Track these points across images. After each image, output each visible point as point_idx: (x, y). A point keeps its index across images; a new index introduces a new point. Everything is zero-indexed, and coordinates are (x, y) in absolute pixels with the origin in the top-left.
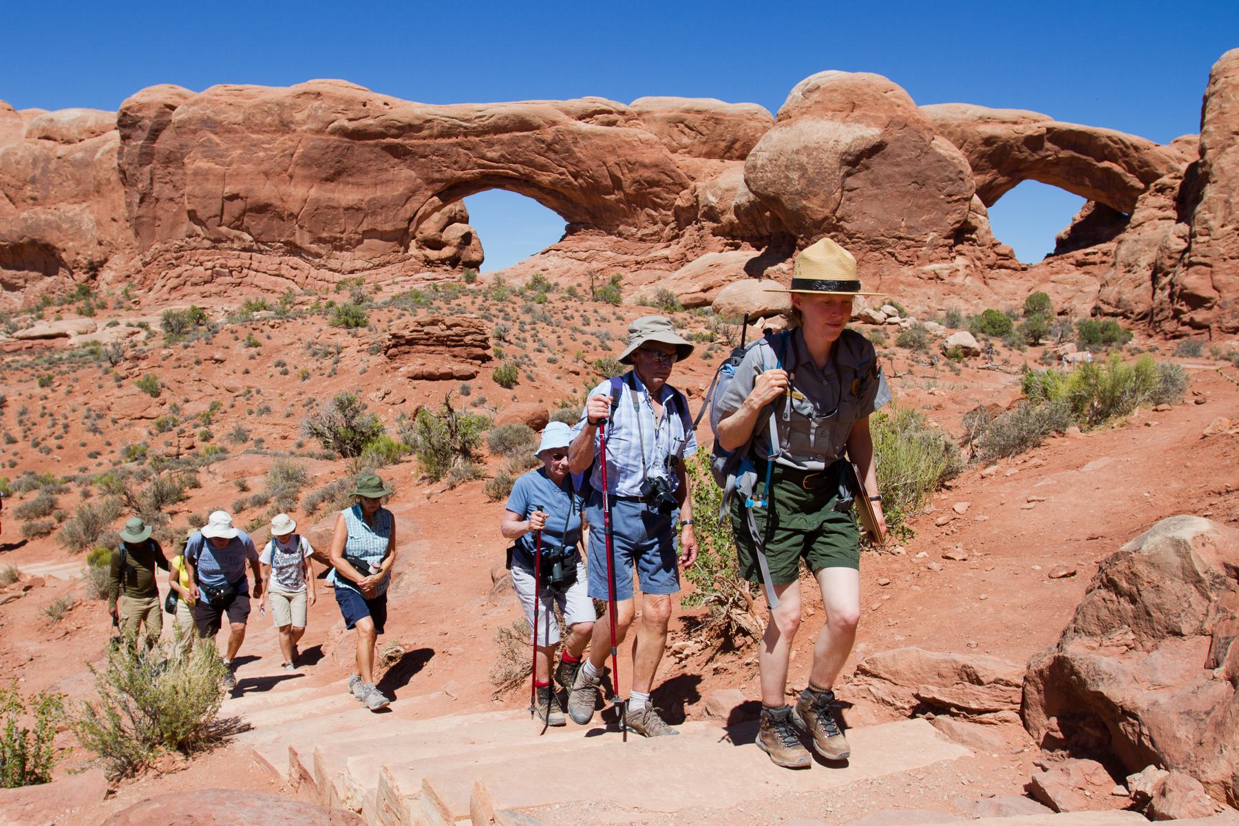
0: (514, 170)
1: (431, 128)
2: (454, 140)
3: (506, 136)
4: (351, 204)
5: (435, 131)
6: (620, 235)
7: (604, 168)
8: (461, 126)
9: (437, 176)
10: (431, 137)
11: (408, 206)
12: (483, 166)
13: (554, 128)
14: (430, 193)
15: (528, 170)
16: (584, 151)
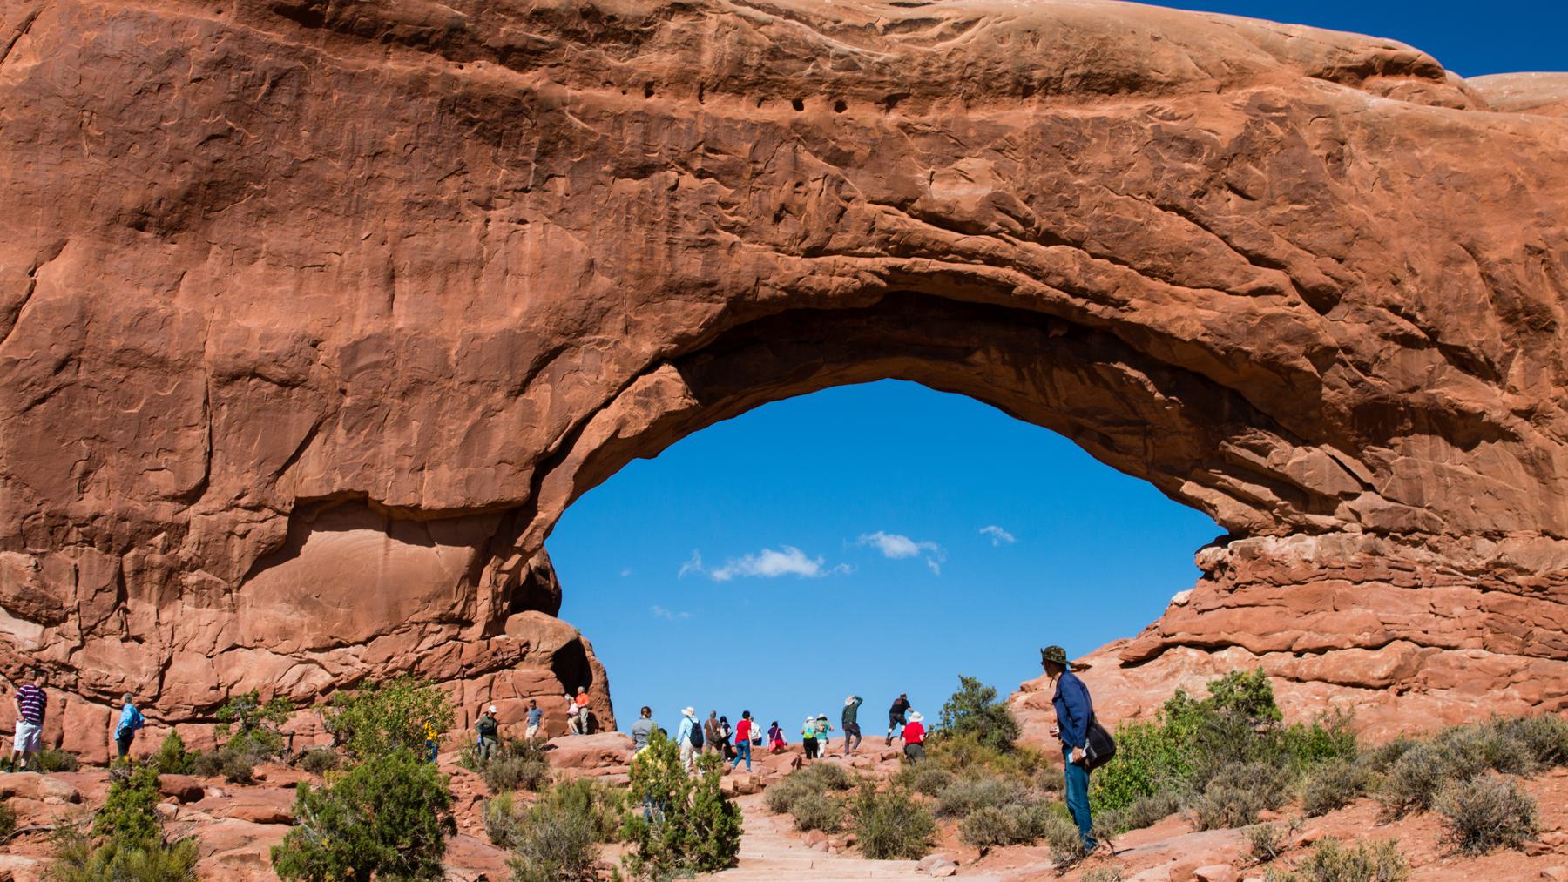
0: (1035, 272)
1: (690, 44)
2: (779, 112)
3: (1022, 116)
4: (255, 351)
5: (707, 58)
6: (1492, 576)
7: (1472, 269)
8: (818, 52)
9: (692, 266)
10: (683, 81)
11: (541, 393)
12: (905, 250)
13: (1241, 95)
14: (647, 348)
15: (1104, 276)
16: (1378, 194)
